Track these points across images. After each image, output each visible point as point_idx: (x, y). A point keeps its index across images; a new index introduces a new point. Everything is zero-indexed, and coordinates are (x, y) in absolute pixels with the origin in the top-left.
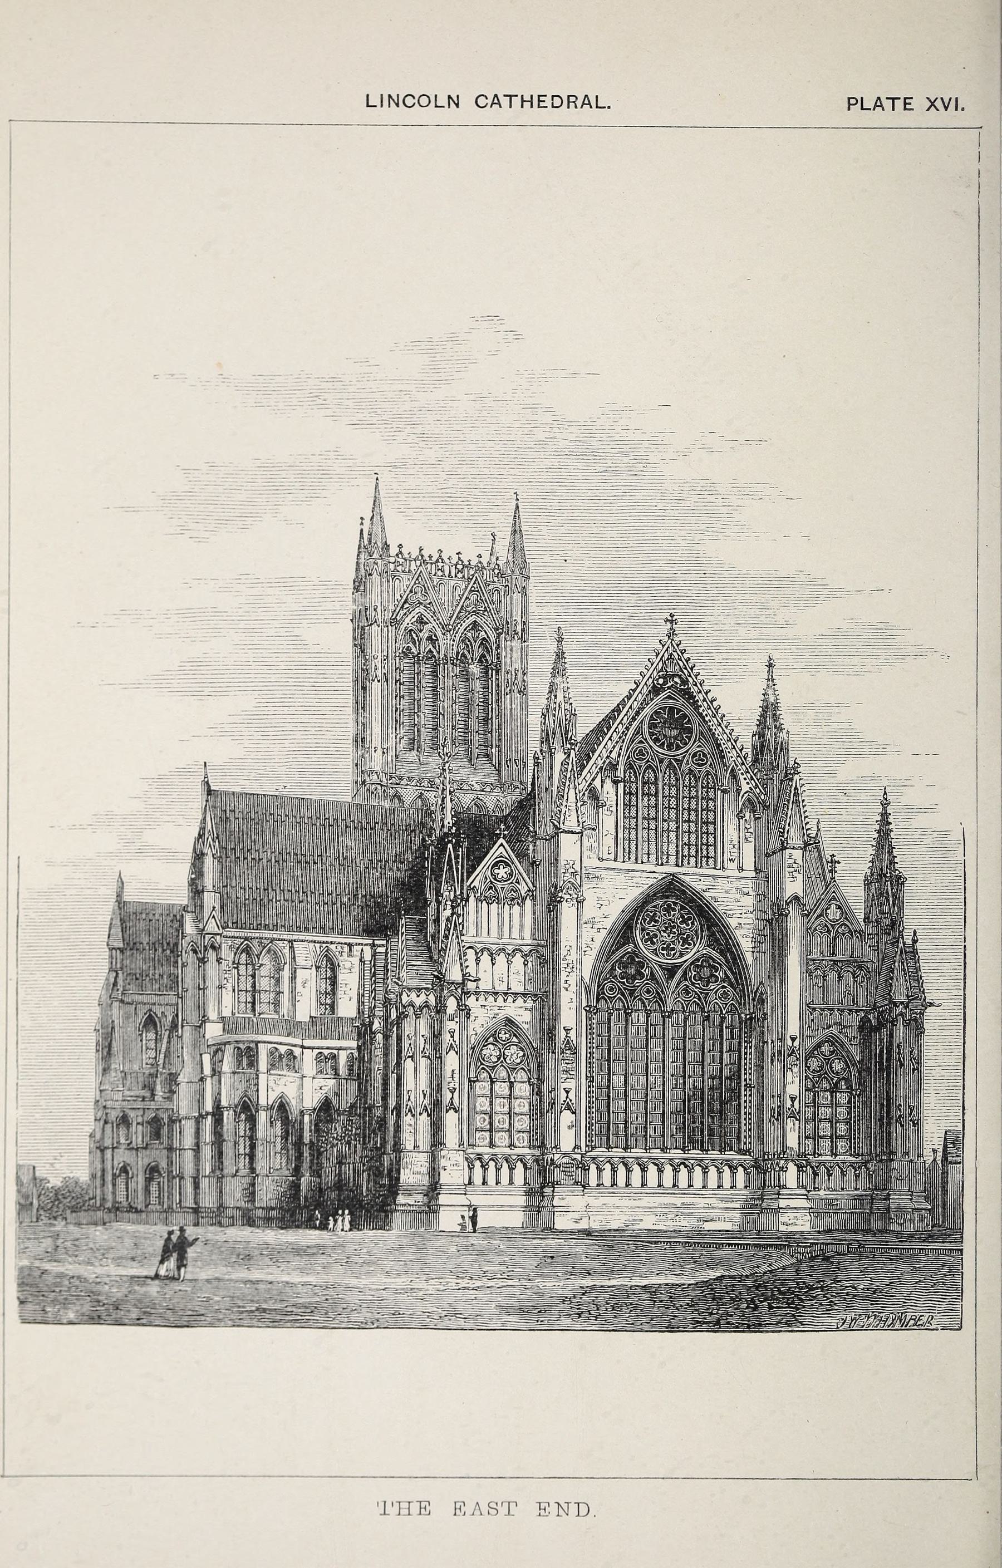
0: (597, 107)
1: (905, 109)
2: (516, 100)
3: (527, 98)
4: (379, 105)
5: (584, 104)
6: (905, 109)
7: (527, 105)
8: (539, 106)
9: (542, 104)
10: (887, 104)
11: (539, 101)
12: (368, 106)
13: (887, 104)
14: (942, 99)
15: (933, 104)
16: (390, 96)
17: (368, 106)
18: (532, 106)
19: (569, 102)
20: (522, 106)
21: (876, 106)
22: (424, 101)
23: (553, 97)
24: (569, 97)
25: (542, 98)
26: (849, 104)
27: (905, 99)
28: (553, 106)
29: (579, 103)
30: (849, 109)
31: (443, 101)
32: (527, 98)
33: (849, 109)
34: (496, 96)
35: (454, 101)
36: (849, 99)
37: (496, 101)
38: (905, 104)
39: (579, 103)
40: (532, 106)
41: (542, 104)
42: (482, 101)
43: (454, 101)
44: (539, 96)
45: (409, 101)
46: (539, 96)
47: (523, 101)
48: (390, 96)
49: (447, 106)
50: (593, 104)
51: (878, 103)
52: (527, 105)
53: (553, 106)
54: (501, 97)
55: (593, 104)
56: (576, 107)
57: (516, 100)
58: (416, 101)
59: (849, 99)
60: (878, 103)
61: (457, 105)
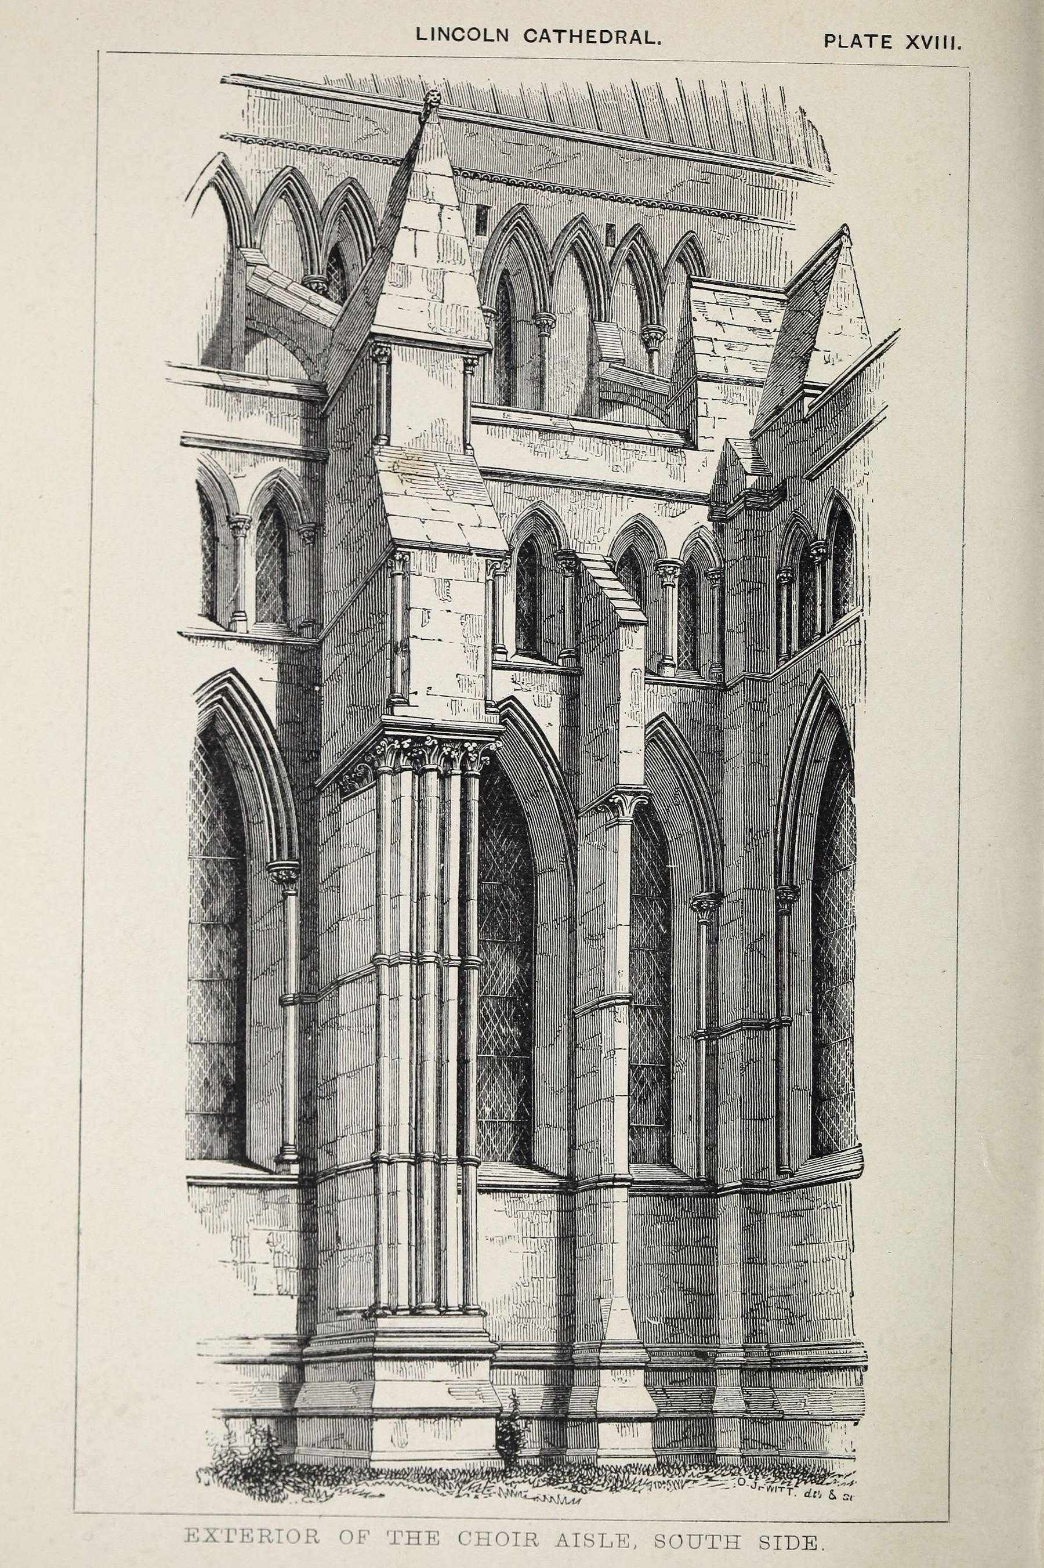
0: (647, 42)
1: (883, 47)
2: (566, 37)
3: (576, 33)
4: (429, 37)
5: (633, 39)
6: (883, 47)
7: (576, 40)
8: (588, 42)
9: (591, 39)
10: (865, 41)
11: (588, 36)
12: (419, 38)
13: (865, 41)
14: (923, 37)
15: (913, 42)
16: (440, 30)
17: (419, 38)
18: (580, 42)
19: (618, 37)
20: (571, 41)
21: (853, 43)
22: (474, 34)
23: (602, 32)
24: (618, 32)
25: (591, 34)
26: (827, 42)
27: (884, 37)
28: (602, 42)
29: (628, 39)
30: (826, 46)
31: (492, 34)
32: (576, 33)
33: (826, 46)
34: (545, 31)
35: (504, 35)
36: (827, 36)
37: (545, 36)
38: (884, 42)
39: (628, 39)
40: (580, 42)
41: (591, 39)
42: (531, 36)
43: (504, 35)
44: (588, 31)
45: (459, 34)
46: (588, 31)
47: (572, 36)
48: (440, 30)
49: (496, 39)
50: (643, 39)
51: (856, 41)
52: (576, 40)
53: (602, 42)
54: (550, 32)
55: (643, 39)
56: (625, 42)
57: (566, 37)
58: (465, 34)
59: (827, 36)
60: (856, 41)
61: (506, 39)
